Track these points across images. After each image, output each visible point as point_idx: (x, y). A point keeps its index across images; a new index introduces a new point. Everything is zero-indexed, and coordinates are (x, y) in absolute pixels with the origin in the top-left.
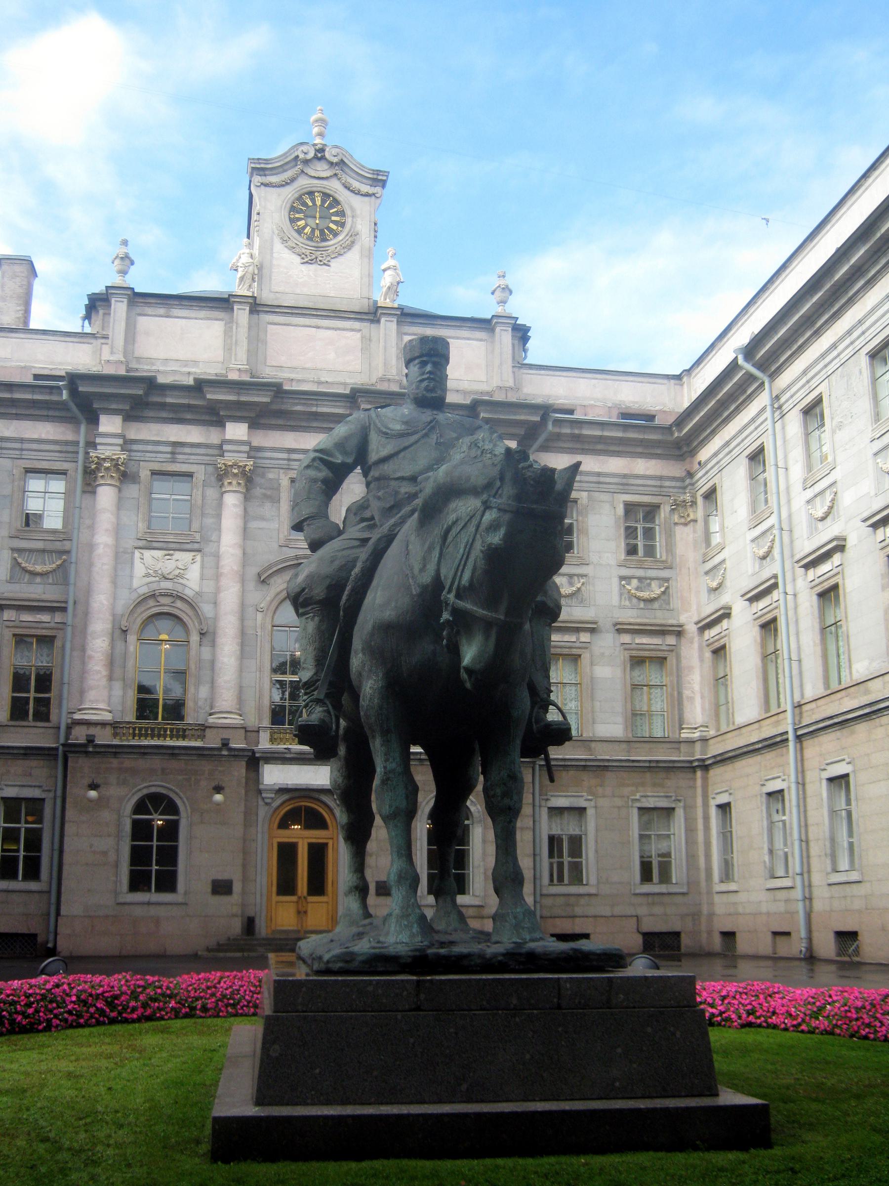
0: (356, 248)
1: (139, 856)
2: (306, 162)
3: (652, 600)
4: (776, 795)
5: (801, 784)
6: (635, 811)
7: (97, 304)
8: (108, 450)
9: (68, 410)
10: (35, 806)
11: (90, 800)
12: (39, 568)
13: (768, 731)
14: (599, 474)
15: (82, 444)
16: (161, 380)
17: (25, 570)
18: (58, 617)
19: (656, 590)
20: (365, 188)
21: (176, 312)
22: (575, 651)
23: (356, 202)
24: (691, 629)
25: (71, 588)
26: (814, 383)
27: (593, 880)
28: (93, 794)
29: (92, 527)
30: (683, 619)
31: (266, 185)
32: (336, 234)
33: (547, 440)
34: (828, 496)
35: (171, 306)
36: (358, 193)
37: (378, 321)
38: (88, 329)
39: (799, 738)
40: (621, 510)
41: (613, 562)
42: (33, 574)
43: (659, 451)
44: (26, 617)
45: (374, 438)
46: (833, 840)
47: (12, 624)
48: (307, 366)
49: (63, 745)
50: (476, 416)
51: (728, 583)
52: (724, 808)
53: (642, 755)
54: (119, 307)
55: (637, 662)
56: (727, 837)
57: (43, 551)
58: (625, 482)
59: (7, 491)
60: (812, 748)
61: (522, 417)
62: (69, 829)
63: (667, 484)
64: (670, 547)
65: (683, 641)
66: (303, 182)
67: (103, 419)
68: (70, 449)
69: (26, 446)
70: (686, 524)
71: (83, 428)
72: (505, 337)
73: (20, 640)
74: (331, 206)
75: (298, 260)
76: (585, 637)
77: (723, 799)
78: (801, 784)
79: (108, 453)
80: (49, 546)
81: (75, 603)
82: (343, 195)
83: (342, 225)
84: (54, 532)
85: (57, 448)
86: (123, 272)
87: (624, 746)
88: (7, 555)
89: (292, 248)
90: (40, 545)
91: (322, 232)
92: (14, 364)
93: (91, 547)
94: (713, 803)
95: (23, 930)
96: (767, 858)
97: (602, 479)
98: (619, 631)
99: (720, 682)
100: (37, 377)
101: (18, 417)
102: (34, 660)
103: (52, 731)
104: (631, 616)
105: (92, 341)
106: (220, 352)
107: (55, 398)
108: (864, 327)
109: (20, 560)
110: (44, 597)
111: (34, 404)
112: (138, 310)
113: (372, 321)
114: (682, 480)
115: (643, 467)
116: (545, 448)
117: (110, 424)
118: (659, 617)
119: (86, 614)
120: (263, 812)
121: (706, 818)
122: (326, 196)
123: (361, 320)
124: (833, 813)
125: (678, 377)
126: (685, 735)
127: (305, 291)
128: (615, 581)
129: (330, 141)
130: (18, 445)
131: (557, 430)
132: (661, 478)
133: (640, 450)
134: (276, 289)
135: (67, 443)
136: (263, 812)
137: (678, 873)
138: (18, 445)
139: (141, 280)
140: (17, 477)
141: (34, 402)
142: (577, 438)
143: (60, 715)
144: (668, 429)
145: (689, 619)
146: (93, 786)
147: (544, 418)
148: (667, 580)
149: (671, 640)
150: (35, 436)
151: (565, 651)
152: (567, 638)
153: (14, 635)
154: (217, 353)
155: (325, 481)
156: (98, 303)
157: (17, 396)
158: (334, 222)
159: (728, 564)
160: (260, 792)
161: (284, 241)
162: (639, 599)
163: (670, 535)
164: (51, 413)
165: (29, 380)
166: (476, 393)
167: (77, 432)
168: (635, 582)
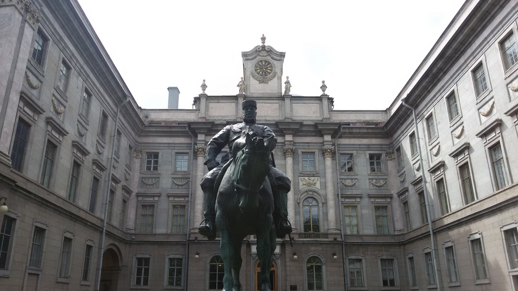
0: (276, 77)
1: (212, 277)
2: (259, 51)
3: (381, 186)
4: (428, 254)
5: (436, 250)
6: (379, 260)
7: (197, 100)
8: (200, 146)
9: (188, 133)
11: (196, 258)
12: (180, 184)
13: (423, 231)
14: (360, 145)
16: (216, 122)
17: (176, 184)
18: (186, 199)
19: (382, 182)
20: (278, 58)
21: (221, 101)
22: (355, 205)
23: (275, 62)
24: (395, 196)
25: (190, 189)
26: (429, 109)
27: (366, 285)
28: (197, 256)
29: (196, 170)
30: (392, 192)
31: (247, 60)
32: (270, 73)
33: (341, 134)
34: (437, 147)
35: (220, 99)
36: (276, 60)
37: (284, 100)
38: (194, 108)
39: (434, 234)
40: (368, 156)
41: (366, 174)
43: (380, 136)
44: (177, 199)
45: (231, 133)
46: (449, 270)
48: (263, 115)
49: (188, 240)
50: (317, 128)
51: (406, 179)
52: (411, 259)
53: (381, 240)
54: (203, 101)
55: (377, 208)
56: (413, 268)
57: (182, 178)
58: (369, 147)
60: (440, 237)
61: (332, 127)
62: (190, 268)
63: (384, 146)
64: (387, 169)
65: (393, 200)
66: (259, 58)
67: (199, 135)
68: (189, 145)
69: (176, 145)
70: (391, 160)
71: (193, 139)
72: (325, 102)
74: (268, 65)
75: (258, 82)
76: (358, 200)
77: (411, 255)
78: (436, 250)
79: (201, 146)
80: (184, 176)
82: (271, 61)
83: (272, 70)
84: (185, 172)
85: (185, 145)
86: (204, 90)
87: (374, 237)
88: (170, 180)
89: (256, 79)
90: (180, 176)
91: (265, 73)
93: (196, 176)
94: (407, 257)
96: (427, 277)
97: (361, 146)
98: (370, 197)
99: (407, 214)
100: (179, 124)
101: (173, 136)
104: (373, 192)
106: (235, 113)
108: (444, 88)
110: (182, 193)
112: (209, 101)
113: (282, 100)
114: (389, 145)
115: (374, 141)
116: (341, 137)
117: (201, 137)
118: (384, 192)
119: (195, 197)
120: (252, 262)
121: (405, 263)
122: (266, 62)
123: (279, 100)
124: (448, 260)
125: (386, 111)
126: (396, 233)
127: (261, 92)
128: (367, 181)
129: (266, 44)
130: (173, 145)
131: (344, 131)
132: (381, 145)
133: (373, 136)
134: (251, 92)
135: (188, 144)
136: (252, 262)
137: (397, 282)
138: (173, 145)
139: (209, 92)
142: (351, 133)
144: (383, 128)
145: (394, 192)
146: (197, 254)
147: (339, 127)
148: (386, 179)
149: (389, 200)
151: (352, 205)
152: (352, 200)
154: (234, 113)
155: (214, 148)
158: (269, 70)
159: (406, 173)
160: (251, 255)
161: (253, 77)
162: (376, 186)
163: (386, 164)
166: (316, 120)
168: (374, 181)
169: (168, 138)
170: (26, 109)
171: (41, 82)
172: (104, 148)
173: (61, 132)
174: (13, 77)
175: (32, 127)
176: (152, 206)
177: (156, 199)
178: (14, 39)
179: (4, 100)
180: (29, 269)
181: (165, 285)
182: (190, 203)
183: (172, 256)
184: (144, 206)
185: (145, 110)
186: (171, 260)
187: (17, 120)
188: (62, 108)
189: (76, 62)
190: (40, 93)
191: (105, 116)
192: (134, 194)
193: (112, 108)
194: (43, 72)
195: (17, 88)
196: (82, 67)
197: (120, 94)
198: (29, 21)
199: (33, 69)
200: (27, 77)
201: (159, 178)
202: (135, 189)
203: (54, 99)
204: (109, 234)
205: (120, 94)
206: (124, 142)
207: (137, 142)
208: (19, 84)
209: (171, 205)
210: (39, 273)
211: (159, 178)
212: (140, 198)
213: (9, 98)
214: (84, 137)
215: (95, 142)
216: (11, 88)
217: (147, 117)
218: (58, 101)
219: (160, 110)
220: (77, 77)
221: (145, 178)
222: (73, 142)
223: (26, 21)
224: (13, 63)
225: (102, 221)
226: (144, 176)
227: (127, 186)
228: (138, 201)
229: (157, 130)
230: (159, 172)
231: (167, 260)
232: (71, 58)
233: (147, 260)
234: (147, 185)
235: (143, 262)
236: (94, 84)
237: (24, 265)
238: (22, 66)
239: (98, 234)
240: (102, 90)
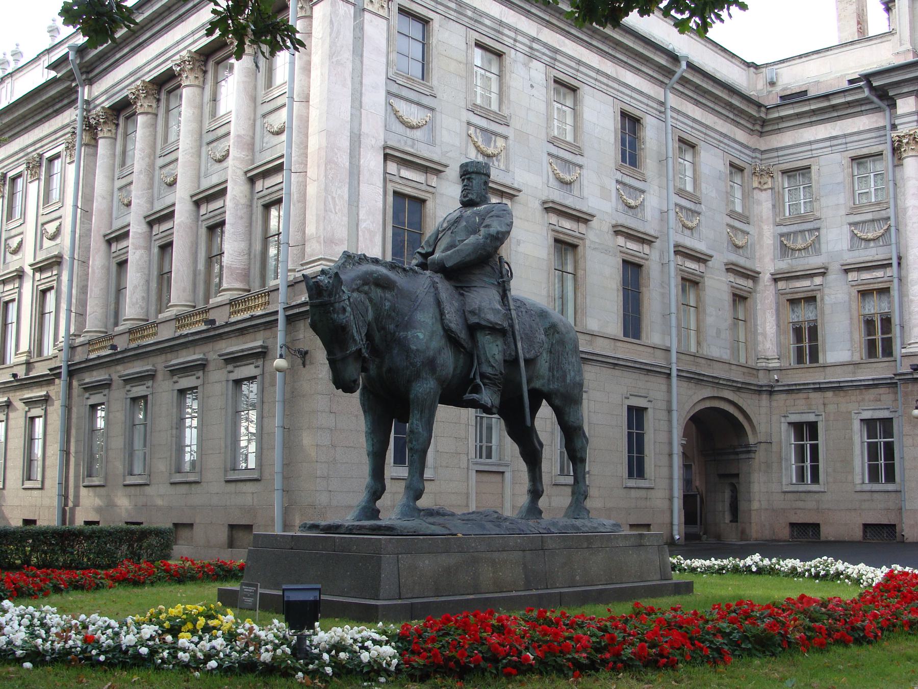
9: (872, 102)
10: (887, 424)
15: (888, 127)
18: (889, 272)
42: (868, 240)
44: (866, 276)
47: (854, 283)
57: (873, 220)
59: (840, 178)
67: (899, 102)
68: (882, 133)
73: (864, 294)
79: (906, 131)
80: (877, 216)
81: (900, 258)
85: (873, 135)
88: (846, 229)
90: (869, 217)
92: (833, 76)
93: (905, 210)
95: (886, 522)
100: (851, 82)
101: (839, 118)
102: (875, 307)
103: (893, 363)
105: (890, 38)
107: (861, 96)
109: (856, 232)
110: (876, 258)
111: (849, 104)
130: (844, 141)
135: (878, 129)
138: (844, 141)
140: (846, 165)
141: (848, 103)
143: (898, 350)
150: (856, 130)
153: (859, 292)
156: (890, 5)
157: (835, 101)
164: (863, 108)
165: (845, 85)
167: (885, 118)
169: (829, 126)
170: (405, 173)
171: (432, 109)
172: (643, 192)
173: (503, 192)
174: (360, 124)
175: (428, 203)
176: (811, 300)
177: (818, 280)
178: (347, 55)
179: (351, 174)
180: (477, 464)
181: (858, 480)
182: (896, 281)
183: (867, 415)
184: (793, 302)
185: (767, 65)
186: (869, 424)
187: (390, 198)
188: (500, 143)
189: (512, 34)
190: (432, 130)
191: (630, 123)
192: (766, 278)
193: (649, 97)
194: (431, 88)
195: (373, 142)
196: (534, 39)
197: (662, 60)
198: (370, 7)
199: (405, 93)
200: (396, 112)
201: (818, 229)
202: (767, 262)
203: (472, 131)
204: (696, 379)
205: (662, 60)
206: (712, 161)
207: (755, 150)
208: (375, 133)
209: (854, 292)
210: (501, 469)
211: (818, 229)
212: (781, 285)
213: (359, 166)
214: (576, 186)
215: (613, 186)
216: (360, 147)
217: (772, 84)
218: (483, 130)
219: (800, 57)
220: (526, 65)
221: (787, 235)
222: (544, 202)
223: (364, 10)
224: (353, 101)
225: (668, 350)
226: (785, 230)
227: (742, 261)
228: (779, 293)
229: (813, 107)
230: (818, 214)
231: (857, 425)
232: (499, 32)
233: (813, 428)
234: (793, 250)
235: (806, 431)
236: (579, 62)
237: (464, 458)
238: (375, 96)
239: (662, 380)
240: (608, 67)
